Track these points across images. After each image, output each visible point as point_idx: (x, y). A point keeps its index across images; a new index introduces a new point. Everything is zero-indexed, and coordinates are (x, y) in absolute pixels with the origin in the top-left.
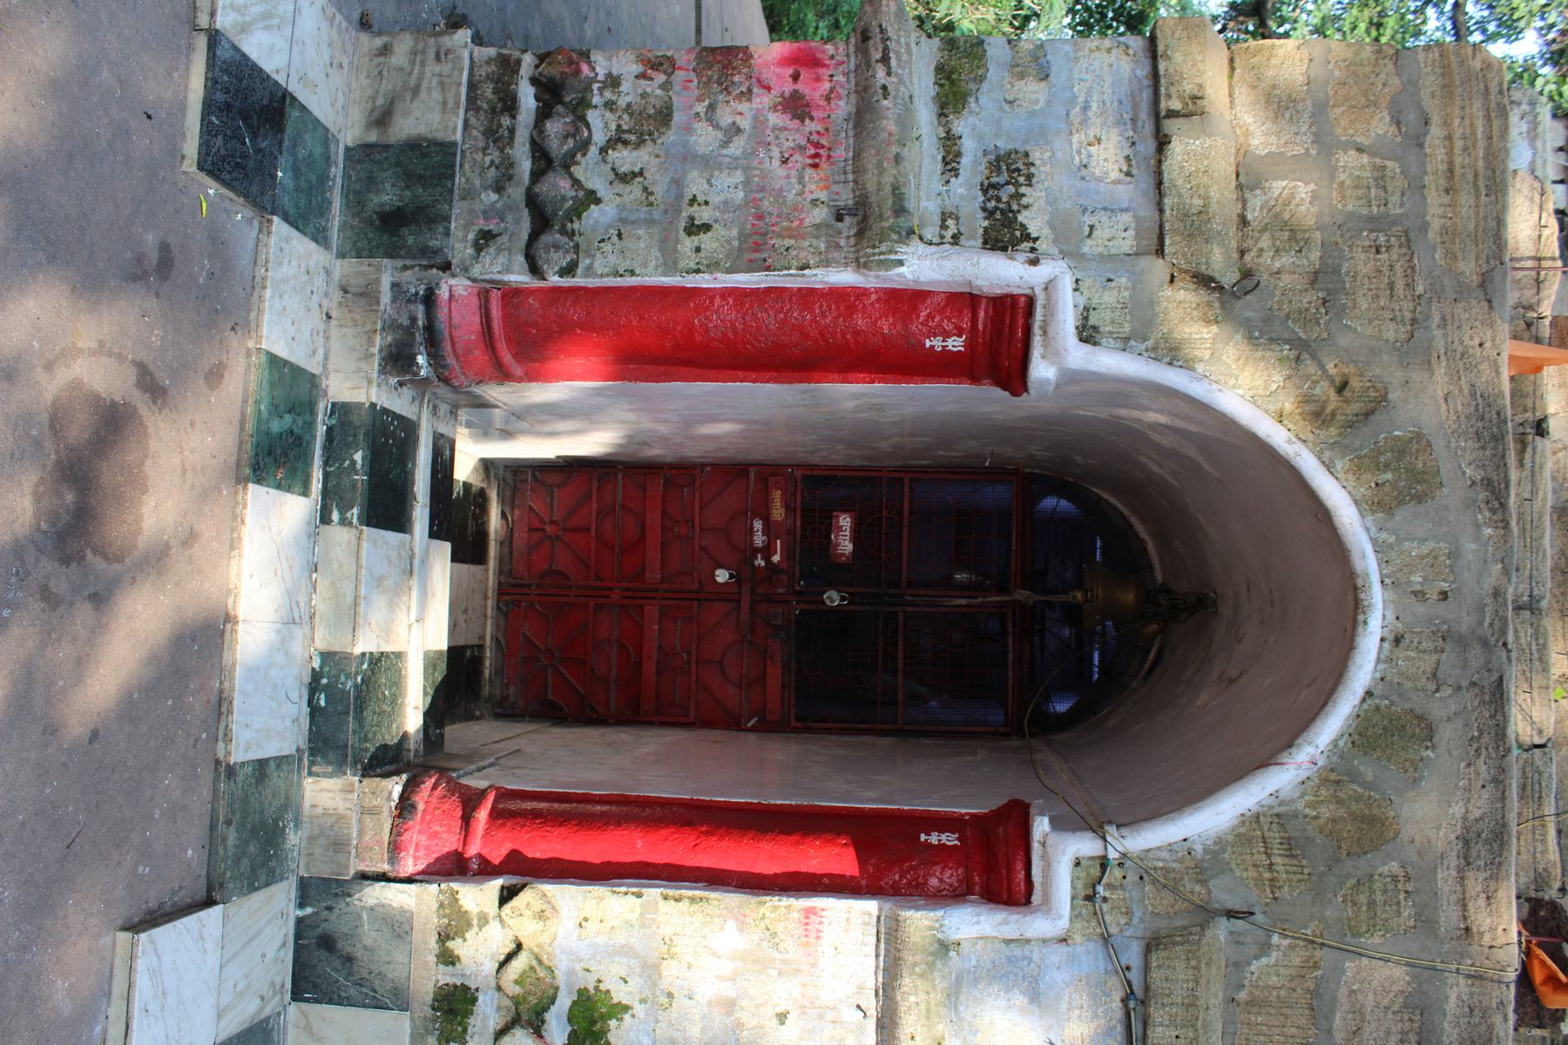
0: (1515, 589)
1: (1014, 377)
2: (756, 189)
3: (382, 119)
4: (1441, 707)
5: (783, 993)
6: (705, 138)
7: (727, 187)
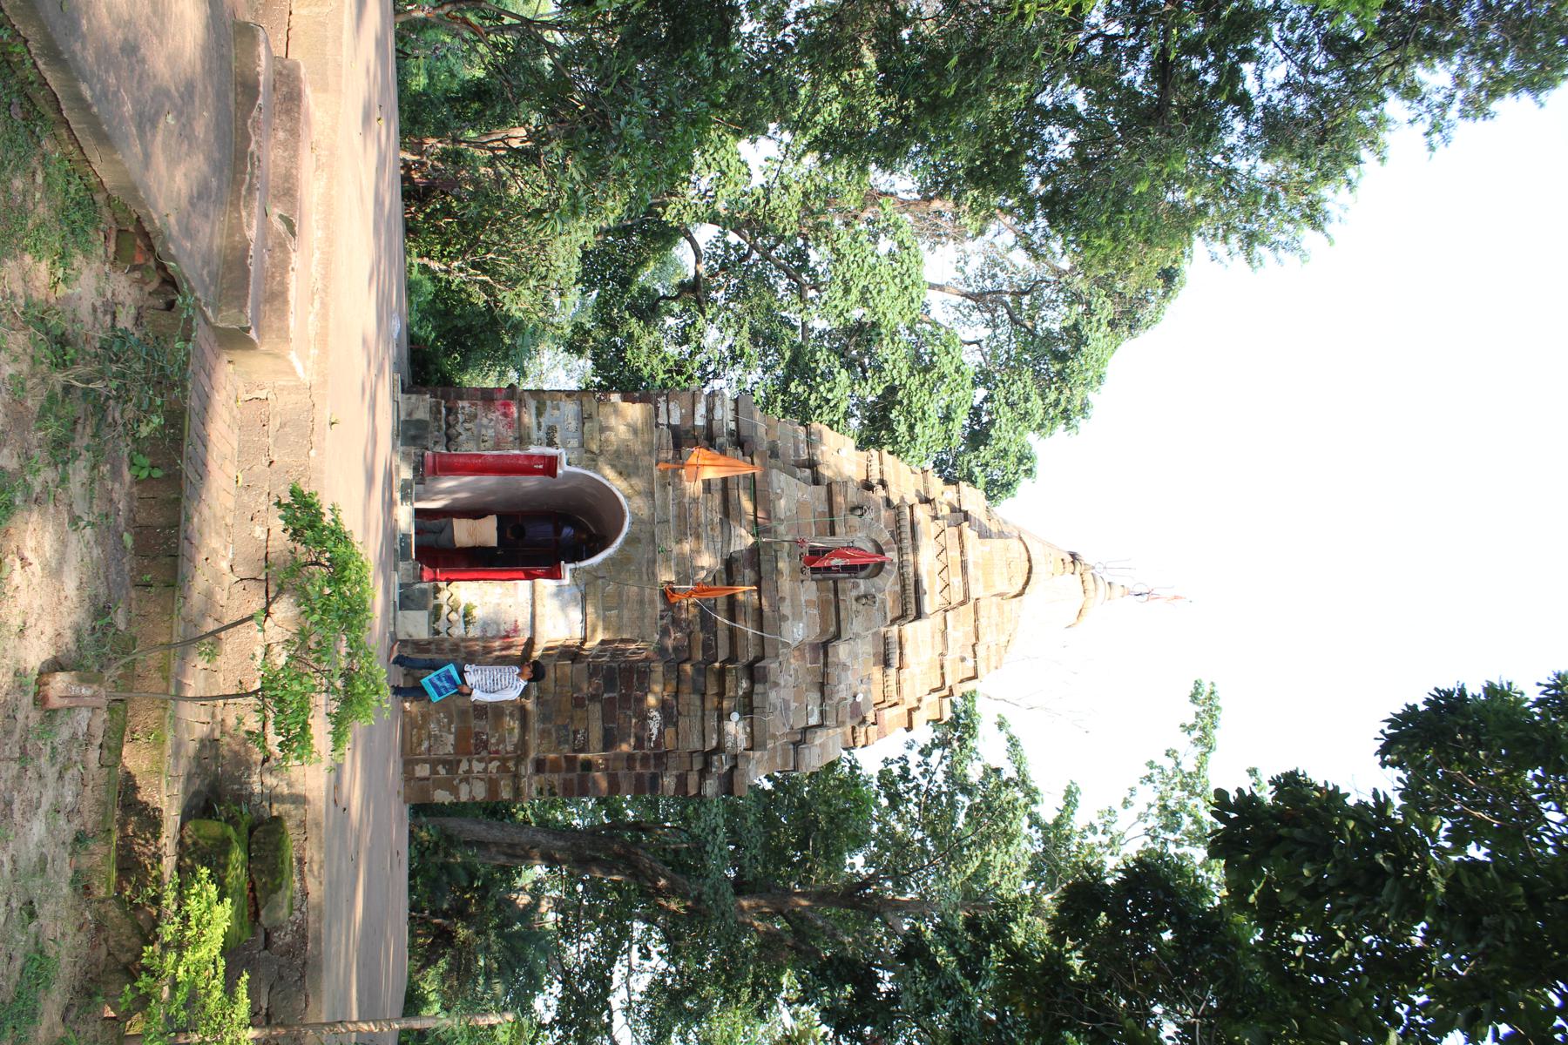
0: (659, 514)
1: (553, 474)
2: (497, 433)
3: (410, 414)
4: (642, 536)
5: (510, 601)
6: (485, 421)
7: (491, 432)
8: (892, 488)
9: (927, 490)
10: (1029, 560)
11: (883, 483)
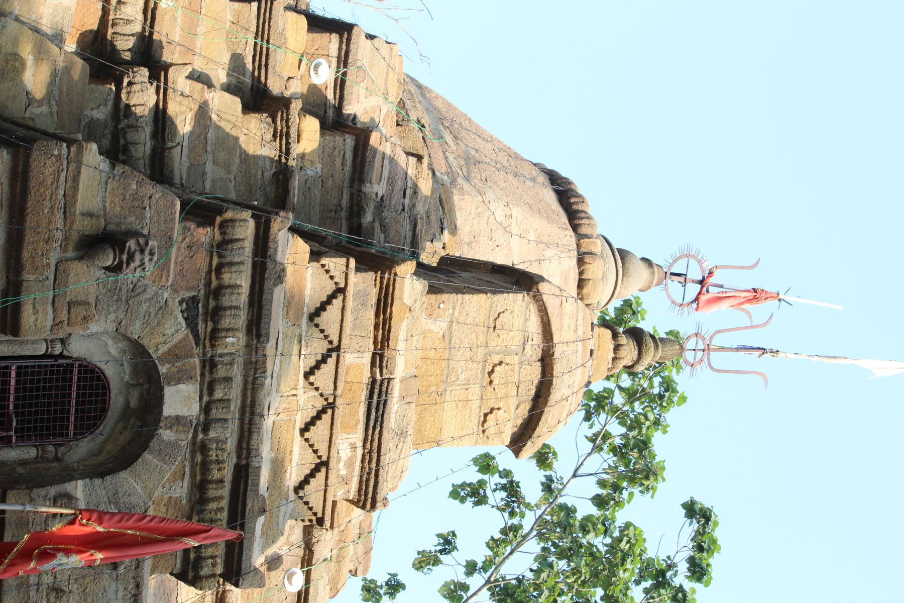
8: (179, 79)
9: (262, 57)
10: (546, 360)
11: (149, 55)
